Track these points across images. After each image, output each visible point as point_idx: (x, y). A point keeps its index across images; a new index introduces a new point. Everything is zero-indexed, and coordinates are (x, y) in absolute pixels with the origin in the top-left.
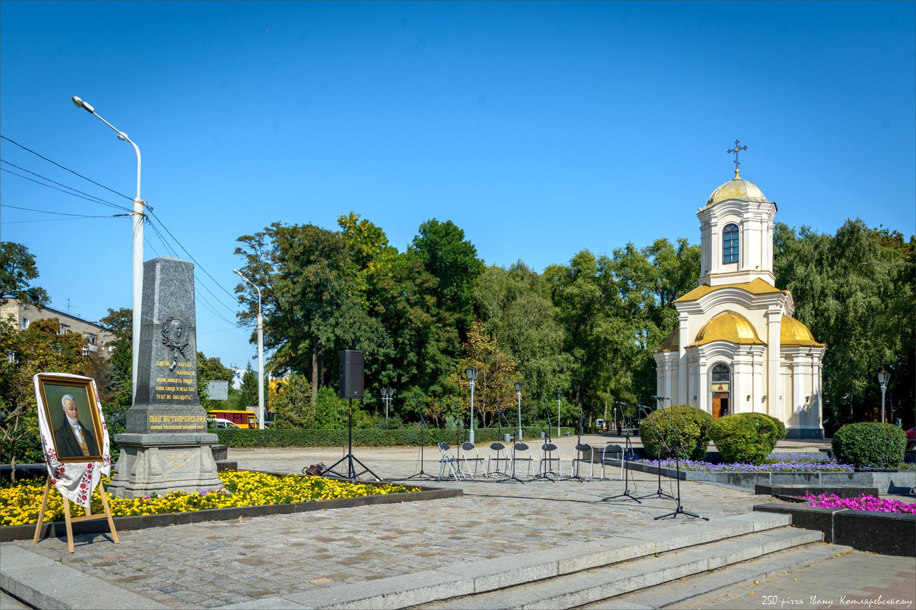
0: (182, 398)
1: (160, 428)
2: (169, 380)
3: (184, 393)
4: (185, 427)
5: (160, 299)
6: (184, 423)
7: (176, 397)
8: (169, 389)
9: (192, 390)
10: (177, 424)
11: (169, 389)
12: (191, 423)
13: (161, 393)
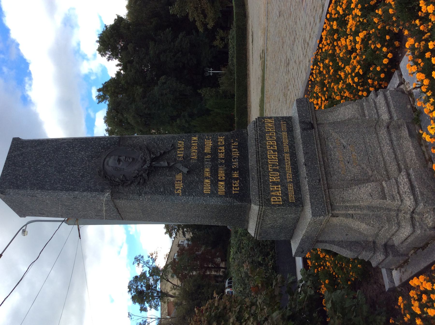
0: (236, 153)
1: (291, 187)
2: (207, 174)
3: (228, 152)
4: (286, 149)
5: (67, 190)
6: (280, 151)
7: (236, 164)
8: (221, 174)
9: (221, 139)
10: (281, 161)
11: (221, 174)
12: (279, 141)
13: (229, 186)
